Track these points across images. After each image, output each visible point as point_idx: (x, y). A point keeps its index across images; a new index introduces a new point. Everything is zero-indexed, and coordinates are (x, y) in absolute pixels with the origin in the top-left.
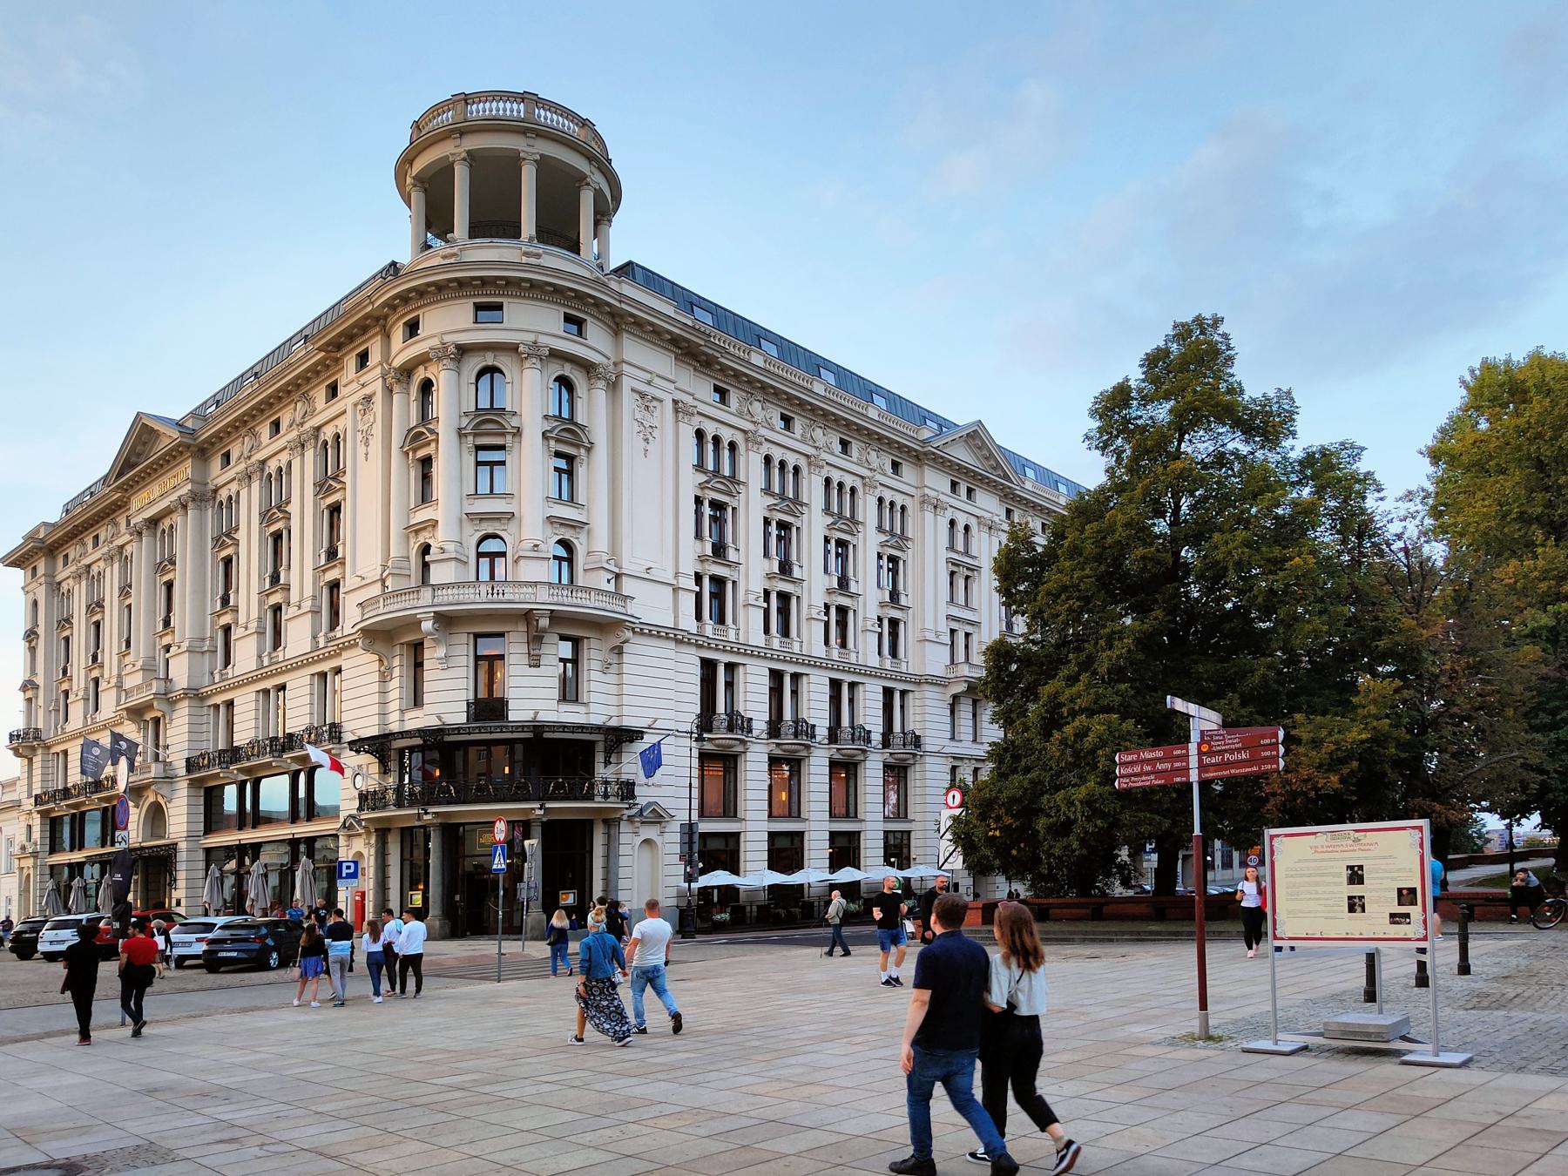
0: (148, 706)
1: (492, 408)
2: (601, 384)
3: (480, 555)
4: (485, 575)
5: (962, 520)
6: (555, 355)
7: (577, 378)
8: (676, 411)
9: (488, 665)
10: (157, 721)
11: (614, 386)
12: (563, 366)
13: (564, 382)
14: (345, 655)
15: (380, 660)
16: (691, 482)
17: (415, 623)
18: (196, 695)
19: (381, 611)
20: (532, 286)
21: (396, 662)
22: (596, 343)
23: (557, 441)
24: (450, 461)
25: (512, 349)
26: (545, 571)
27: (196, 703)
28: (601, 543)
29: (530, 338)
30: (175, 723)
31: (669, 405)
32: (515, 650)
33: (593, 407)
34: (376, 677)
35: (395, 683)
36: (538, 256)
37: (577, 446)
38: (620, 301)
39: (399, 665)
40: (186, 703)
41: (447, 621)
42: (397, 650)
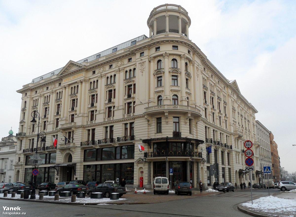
0: (70, 128)
1: (174, 67)
2: (192, 65)
3: (173, 99)
4: (159, 104)
6: (187, 58)
9: (177, 123)
10: (70, 133)
12: (187, 60)
13: (186, 64)
14: (136, 120)
15: (148, 121)
17: (163, 113)
19: (154, 110)
20: (176, 42)
21: (154, 122)
23: (187, 76)
24: (167, 79)
25: (180, 55)
26: (185, 103)
27: (83, 129)
28: (193, 99)
29: (183, 54)
30: (76, 133)
32: (183, 121)
33: (191, 69)
34: (147, 125)
36: (183, 37)
37: (189, 77)
38: (197, 48)
39: (154, 123)
40: (81, 129)
41: (170, 113)
42: (154, 119)
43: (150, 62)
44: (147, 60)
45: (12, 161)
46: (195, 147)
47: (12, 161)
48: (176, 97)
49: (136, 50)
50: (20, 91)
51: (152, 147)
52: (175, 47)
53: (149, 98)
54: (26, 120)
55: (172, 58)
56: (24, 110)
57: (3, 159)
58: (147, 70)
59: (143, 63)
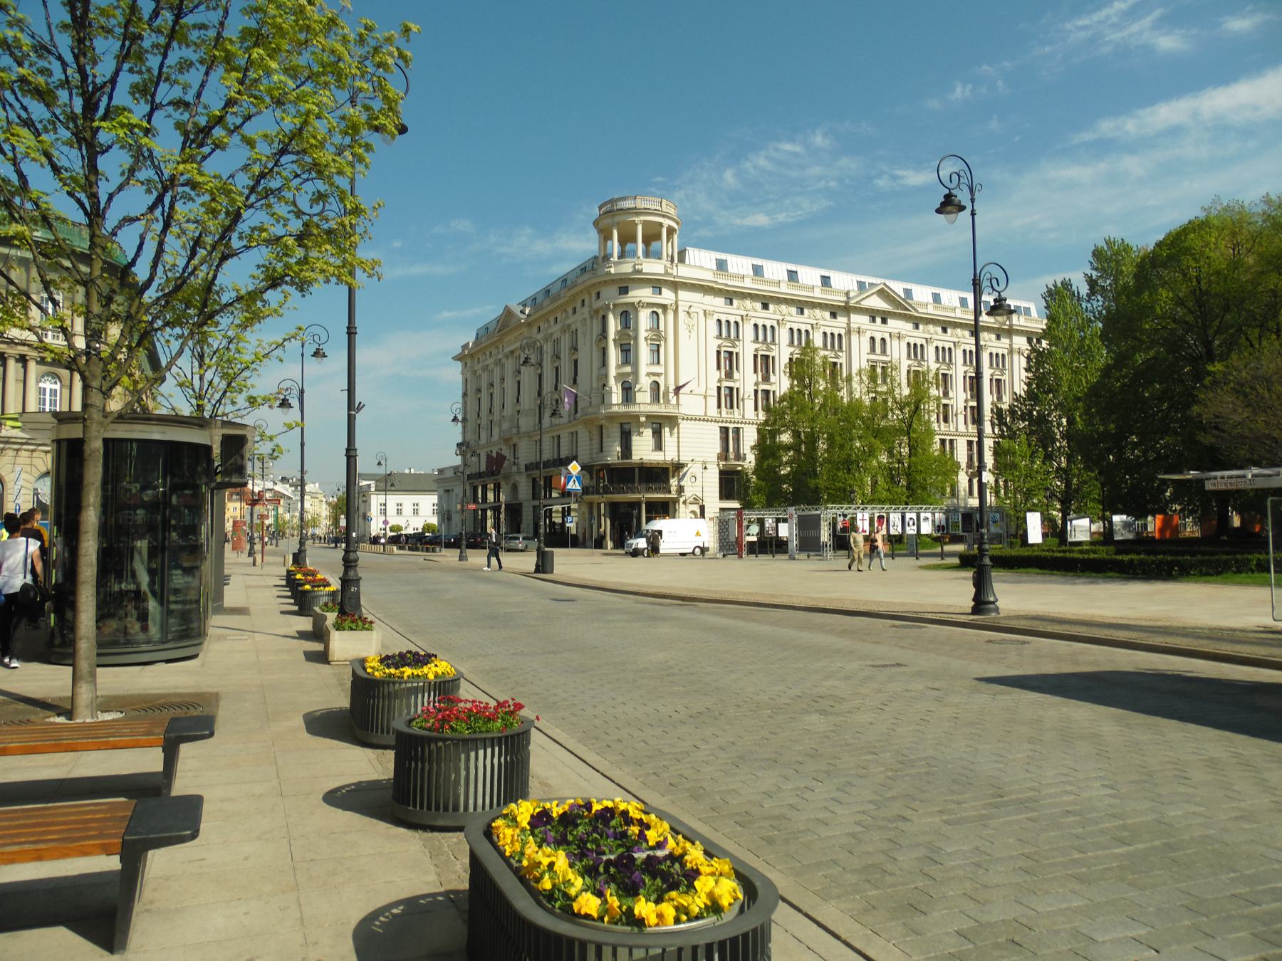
5: (878, 338)
7: (660, 311)
8: (705, 315)
10: (515, 445)
11: (676, 311)
16: (714, 344)
18: (528, 435)
22: (667, 296)
31: (701, 313)
35: (594, 442)
41: (612, 417)
43: (591, 317)
44: (587, 315)
45: (457, 496)
46: (671, 474)
47: (457, 496)
48: (626, 385)
49: (573, 296)
50: (458, 358)
51: (595, 476)
52: (624, 291)
53: (591, 389)
54: (468, 417)
55: (620, 310)
56: (465, 395)
57: (448, 491)
58: (588, 332)
59: (585, 319)
